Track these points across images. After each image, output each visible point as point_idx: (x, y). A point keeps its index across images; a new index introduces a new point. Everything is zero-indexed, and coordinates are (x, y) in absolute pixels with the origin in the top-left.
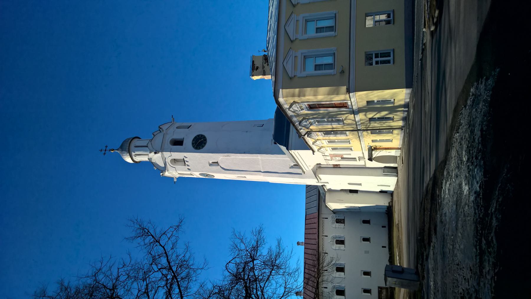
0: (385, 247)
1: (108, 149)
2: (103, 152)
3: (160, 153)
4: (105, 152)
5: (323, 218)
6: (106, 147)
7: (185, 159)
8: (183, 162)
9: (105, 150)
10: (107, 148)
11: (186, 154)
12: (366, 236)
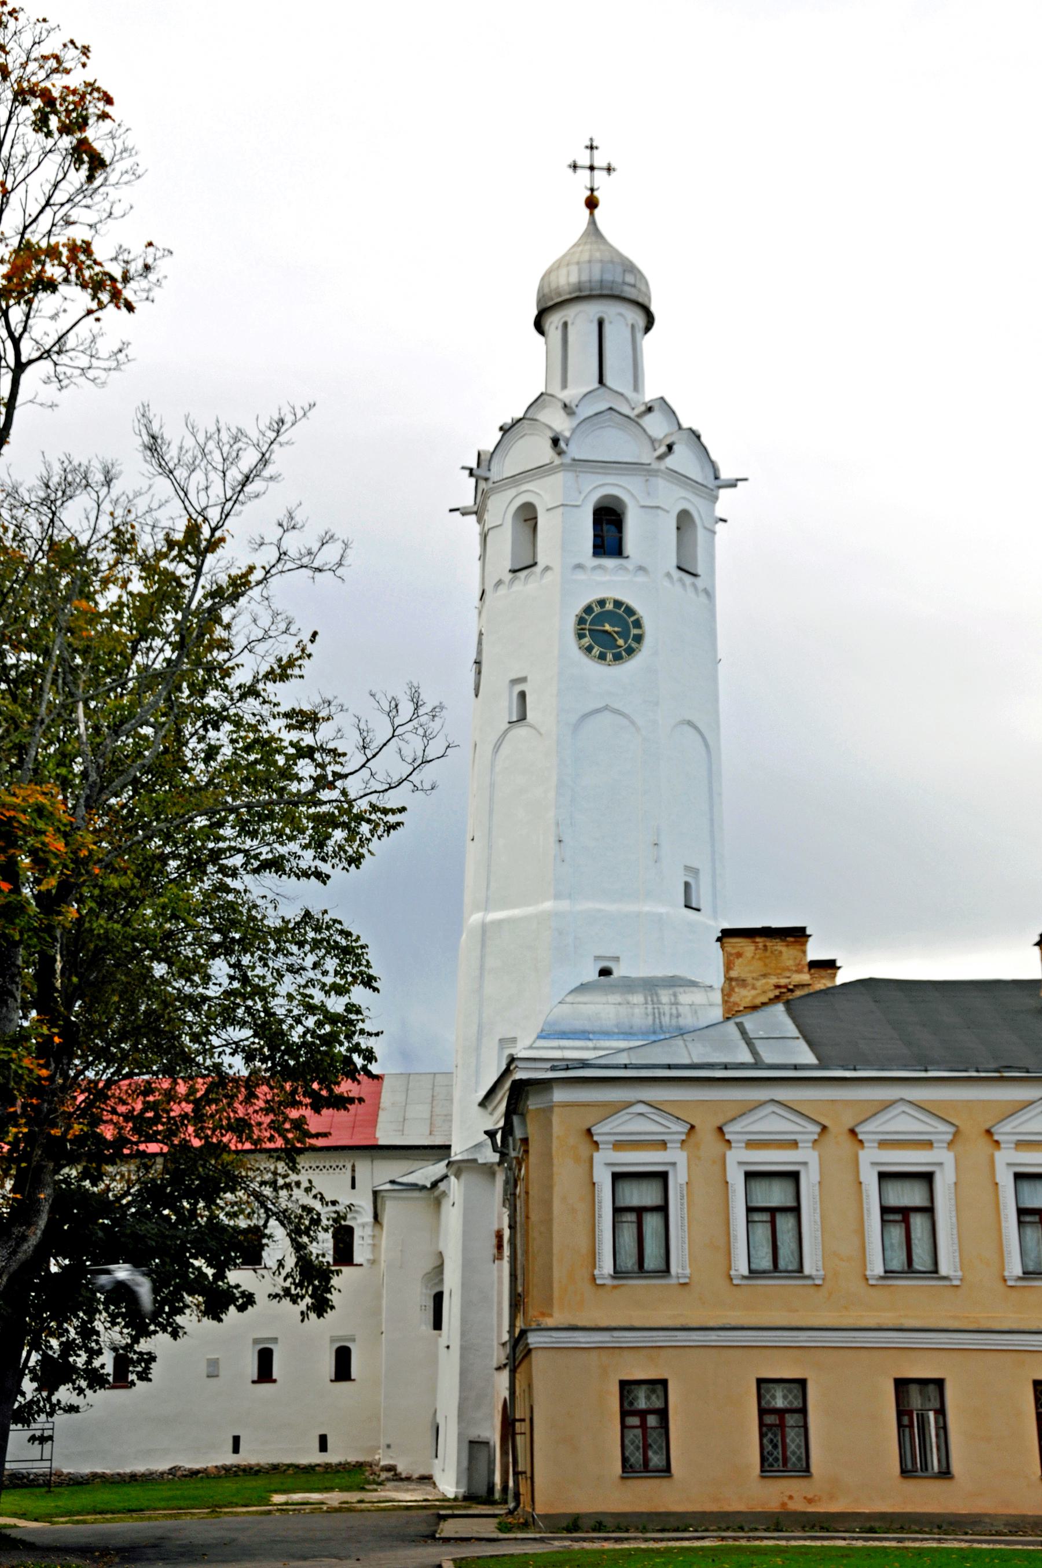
0: (236, 1450)
1: (600, 175)
2: (584, 160)
5: (353, 1166)
6: (609, 169)
7: (538, 569)
10: (605, 173)
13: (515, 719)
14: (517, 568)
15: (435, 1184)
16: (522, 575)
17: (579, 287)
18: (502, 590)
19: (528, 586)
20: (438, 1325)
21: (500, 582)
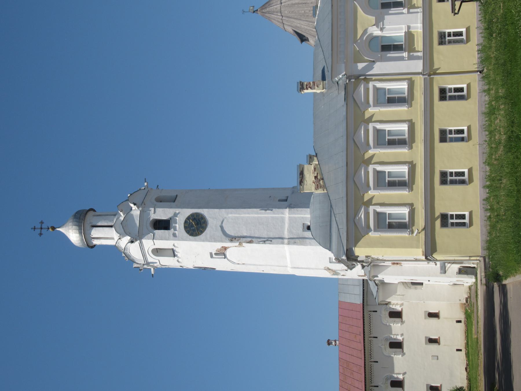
0: (460, 350)
1: (44, 226)
2: (38, 231)
3: (139, 241)
4: (41, 232)
5: (369, 311)
6: (42, 223)
7: (175, 248)
8: (173, 253)
9: (41, 228)
11: (176, 243)
12: (434, 346)
13: (224, 257)
14: (173, 255)
15: (376, 285)
16: (176, 253)
17: (80, 233)
18: (180, 260)
19: (179, 252)
20: (421, 284)
21: (178, 261)
